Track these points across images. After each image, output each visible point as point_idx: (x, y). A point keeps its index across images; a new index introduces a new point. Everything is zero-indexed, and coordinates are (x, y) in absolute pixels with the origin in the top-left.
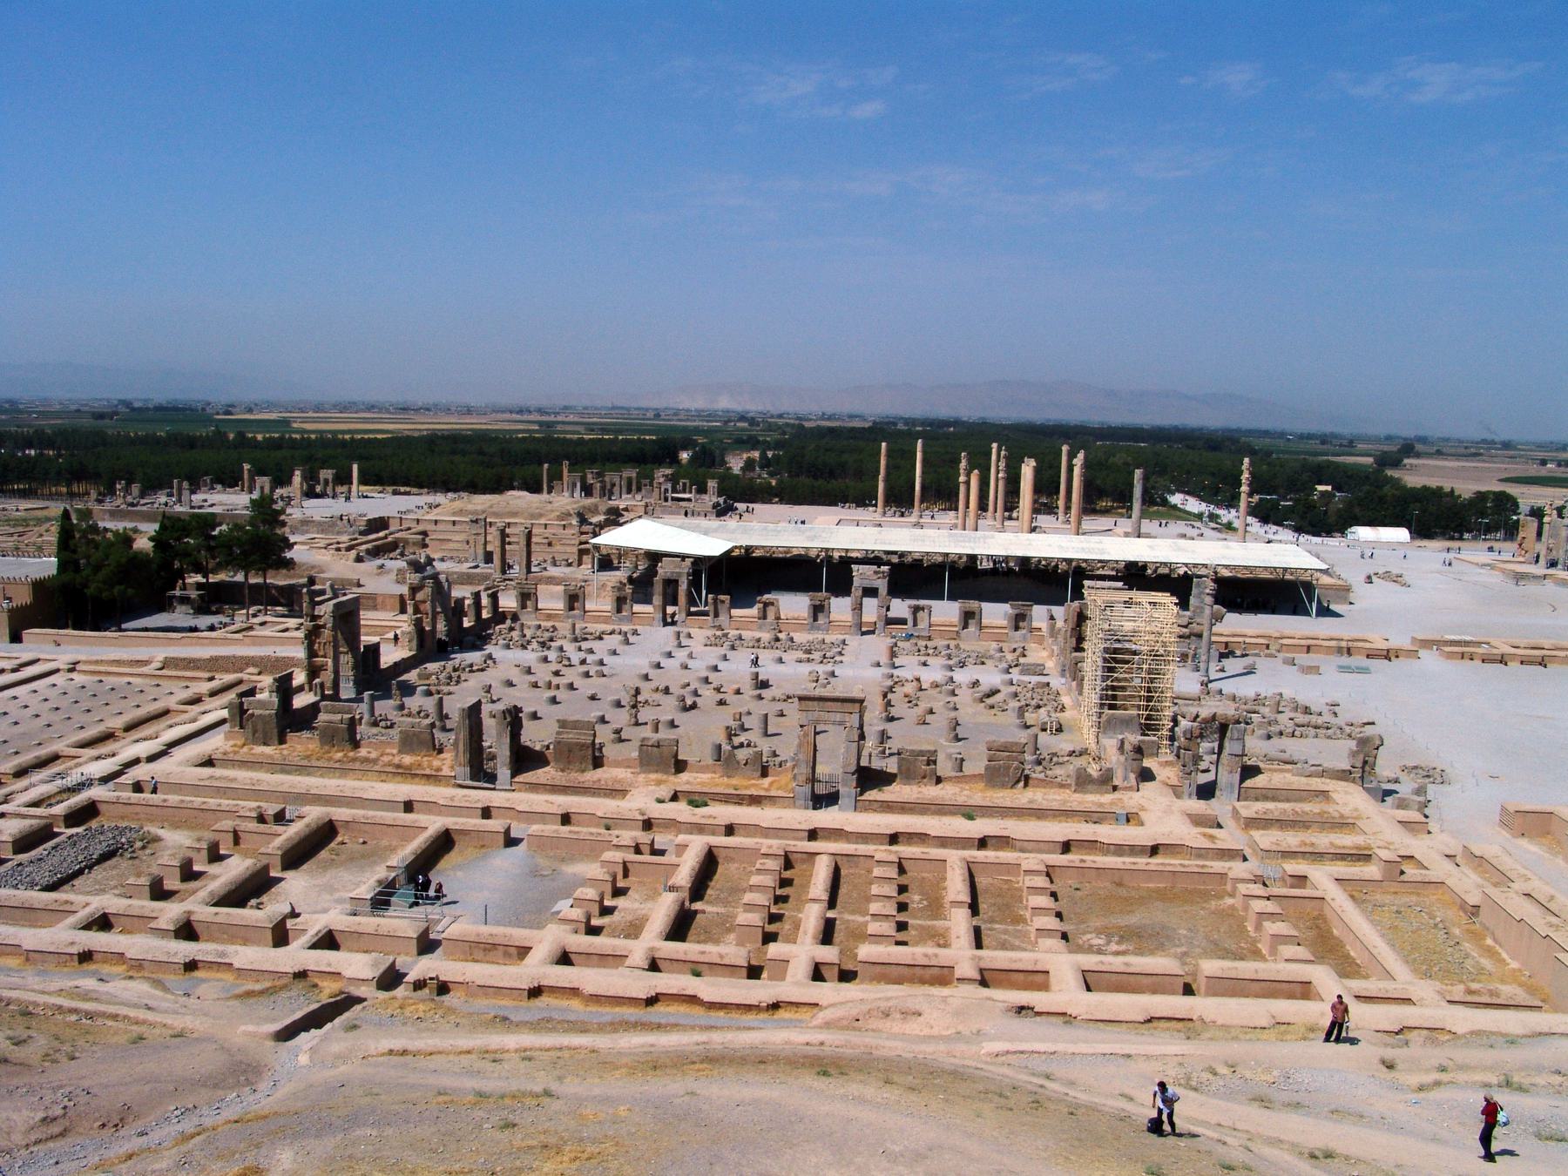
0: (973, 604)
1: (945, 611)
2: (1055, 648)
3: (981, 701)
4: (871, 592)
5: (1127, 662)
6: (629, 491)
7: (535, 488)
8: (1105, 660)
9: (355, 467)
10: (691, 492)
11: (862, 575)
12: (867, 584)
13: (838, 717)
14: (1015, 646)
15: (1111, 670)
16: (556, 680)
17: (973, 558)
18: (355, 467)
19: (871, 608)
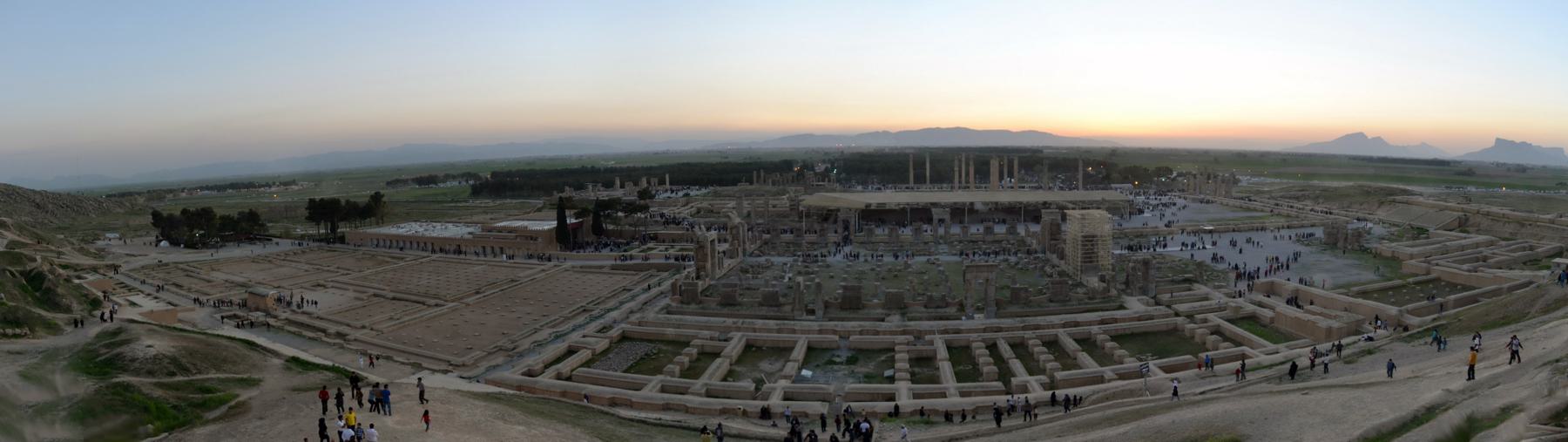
0: (991, 223)
1: (976, 230)
2: (1034, 241)
3: (1012, 267)
4: (941, 221)
5: (1092, 241)
6: (793, 182)
7: (751, 183)
8: (1082, 241)
9: (667, 177)
10: (823, 181)
11: (936, 213)
12: (941, 217)
13: (986, 274)
14: (1012, 242)
15: (1086, 245)
16: (810, 270)
17: (972, 204)
18: (667, 177)
19: (941, 231)
